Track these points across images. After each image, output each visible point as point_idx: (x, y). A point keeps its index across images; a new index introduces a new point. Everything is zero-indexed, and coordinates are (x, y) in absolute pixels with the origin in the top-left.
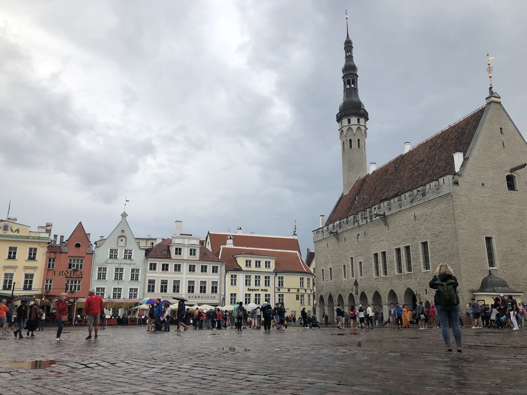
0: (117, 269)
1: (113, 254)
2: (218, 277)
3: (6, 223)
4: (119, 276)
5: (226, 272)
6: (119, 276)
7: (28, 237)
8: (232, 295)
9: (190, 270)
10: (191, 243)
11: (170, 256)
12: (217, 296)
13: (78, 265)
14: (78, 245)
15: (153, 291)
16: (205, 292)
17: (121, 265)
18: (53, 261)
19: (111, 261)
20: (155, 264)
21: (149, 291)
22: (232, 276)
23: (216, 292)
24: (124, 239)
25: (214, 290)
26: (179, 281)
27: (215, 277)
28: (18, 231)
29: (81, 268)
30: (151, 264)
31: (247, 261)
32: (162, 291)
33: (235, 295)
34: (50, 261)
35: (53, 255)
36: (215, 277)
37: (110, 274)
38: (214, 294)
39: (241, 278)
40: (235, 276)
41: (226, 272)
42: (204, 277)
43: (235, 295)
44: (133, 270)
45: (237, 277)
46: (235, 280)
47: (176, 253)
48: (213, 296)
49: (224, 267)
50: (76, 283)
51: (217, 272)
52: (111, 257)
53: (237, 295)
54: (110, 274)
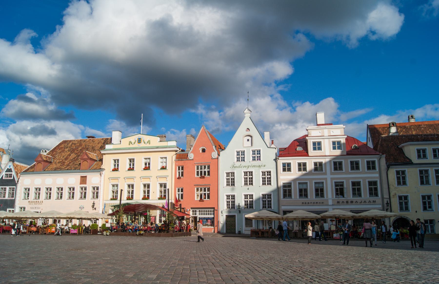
0: (246, 173)
1: (241, 156)
2: (377, 175)
3: (139, 135)
4: (249, 181)
5: (388, 167)
6: (249, 181)
7: (157, 148)
8: (400, 198)
9: (335, 169)
10: (332, 134)
11: (307, 153)
12: (378, 199)
13: (205, 172)
14: (204, 151)
15: (290, 196)
16: (360, 195)
17: (250, 168)
18: (182, 169)
19: (238, 164)
20: (289, 164)
21: (285, 196)
22: (398, 173)
23: (376, 195)
24: (250, 138)
25: (373, 191)
26: (323, 183)
27: (374, 176)
28: (149, 142)
29: (209, 174)
30: (284, 165)
31: (419, 151)
32: (301, 195)
33: (406, 197)
34: (179, 169)
35: (181, 163)
36: (374, 176)
37: (240, 179)
38: (373, 198)
39: (412, 174)
40: (403, 172)
41: (388, 167)
42: (355, 176)
43: (406, 197)
44: (264, 173)
45: (407, 173)
46: (404, 178)
47: (315, 149)
48: (372, 200)
49: (383, 161)
50: (205, 191)
51: (374, 168)
52: (238, 160)
53: (409, 198)
54: (240, 179)
